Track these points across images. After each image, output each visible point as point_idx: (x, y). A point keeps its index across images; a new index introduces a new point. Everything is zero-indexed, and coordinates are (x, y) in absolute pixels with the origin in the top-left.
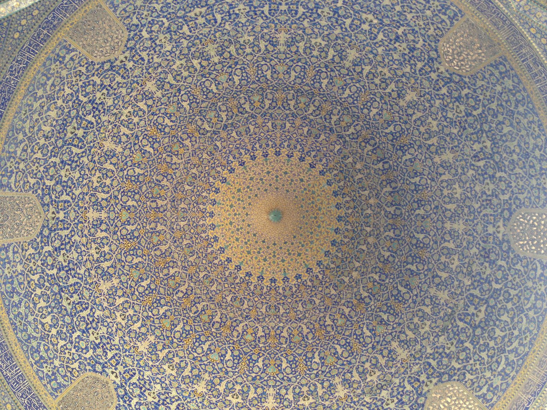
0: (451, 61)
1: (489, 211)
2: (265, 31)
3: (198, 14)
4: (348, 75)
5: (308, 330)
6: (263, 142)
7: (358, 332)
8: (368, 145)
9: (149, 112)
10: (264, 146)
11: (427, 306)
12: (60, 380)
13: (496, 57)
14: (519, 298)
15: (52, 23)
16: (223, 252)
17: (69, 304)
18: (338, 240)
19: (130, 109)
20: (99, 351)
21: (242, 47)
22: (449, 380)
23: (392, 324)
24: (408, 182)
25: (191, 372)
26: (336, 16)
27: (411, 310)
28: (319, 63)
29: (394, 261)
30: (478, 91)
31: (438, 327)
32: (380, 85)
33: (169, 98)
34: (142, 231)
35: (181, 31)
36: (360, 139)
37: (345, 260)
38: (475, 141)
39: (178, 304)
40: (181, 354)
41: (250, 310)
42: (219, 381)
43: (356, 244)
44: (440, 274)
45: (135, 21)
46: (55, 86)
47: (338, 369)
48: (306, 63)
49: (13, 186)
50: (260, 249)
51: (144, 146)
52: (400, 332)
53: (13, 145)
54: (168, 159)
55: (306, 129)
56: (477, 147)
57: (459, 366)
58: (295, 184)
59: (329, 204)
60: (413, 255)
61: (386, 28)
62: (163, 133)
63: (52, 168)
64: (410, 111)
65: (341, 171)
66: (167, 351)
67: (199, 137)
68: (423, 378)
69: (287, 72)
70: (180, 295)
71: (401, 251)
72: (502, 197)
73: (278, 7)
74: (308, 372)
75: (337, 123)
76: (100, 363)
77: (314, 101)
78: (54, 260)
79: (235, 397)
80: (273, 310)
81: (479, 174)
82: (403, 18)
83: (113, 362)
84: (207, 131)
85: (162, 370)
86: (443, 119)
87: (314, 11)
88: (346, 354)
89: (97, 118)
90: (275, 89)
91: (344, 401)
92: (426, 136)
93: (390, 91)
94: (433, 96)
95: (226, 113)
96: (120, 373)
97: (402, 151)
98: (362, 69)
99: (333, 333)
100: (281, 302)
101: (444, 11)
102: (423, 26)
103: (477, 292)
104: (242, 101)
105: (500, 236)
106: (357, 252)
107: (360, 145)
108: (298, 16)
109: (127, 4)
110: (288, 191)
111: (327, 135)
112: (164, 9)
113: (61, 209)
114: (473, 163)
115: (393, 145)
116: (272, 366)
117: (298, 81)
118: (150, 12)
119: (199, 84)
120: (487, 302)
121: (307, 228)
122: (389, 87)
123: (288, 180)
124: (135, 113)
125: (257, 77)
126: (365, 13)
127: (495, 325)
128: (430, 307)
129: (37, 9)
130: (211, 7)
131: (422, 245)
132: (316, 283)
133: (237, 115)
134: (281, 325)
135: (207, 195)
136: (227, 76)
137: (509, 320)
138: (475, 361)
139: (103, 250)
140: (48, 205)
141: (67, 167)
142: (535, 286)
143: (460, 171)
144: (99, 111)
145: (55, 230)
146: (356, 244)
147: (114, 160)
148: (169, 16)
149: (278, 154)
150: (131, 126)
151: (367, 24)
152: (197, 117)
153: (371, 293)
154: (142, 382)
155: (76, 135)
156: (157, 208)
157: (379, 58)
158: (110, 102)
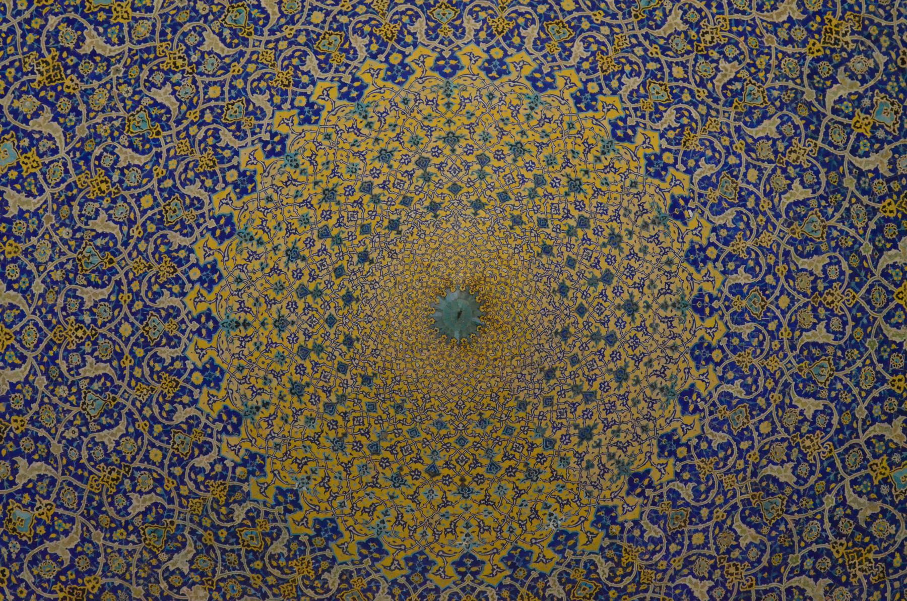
6: (753, 303)
10: (738, 303)
16: (345, 96)
41: (108, 172)
50: (338, 241)
55: (785, 474)
58: (574, 406)
67: (803, 57)
80: (96, 260)
84: (822, 91)
95: (884, 170)
100: (125, 297)
110: (550, 374)
111: (753, 554)
121: (397, 432)
123: (591, 380)
134: (38, 287)
135: (573, 61)
149: (701, 353)
152: (882, 59)
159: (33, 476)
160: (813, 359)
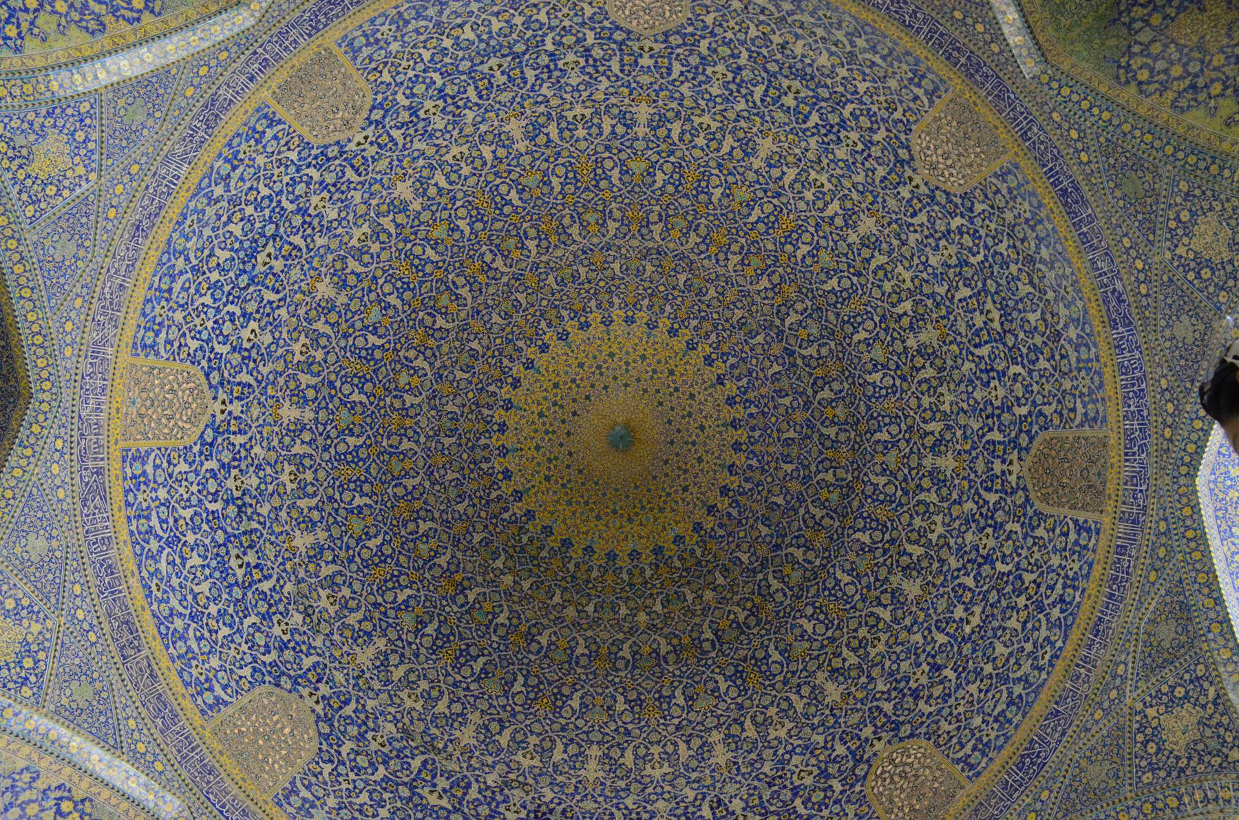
0: (892, 761)
2: (959, 433)
3: (990, 316)
4: (877, 579)
6: (760, 421)
7: (403, 580)
8: (746, 613)
9: (822, 219)
11: (449, 707)
12: (366, 51)
15: (977, 71)
16: (560, 339)
17: (491, 69)
18: (571, 553)
19: (828, 186)
20: (405, 116)
21: (932, 391)
22: (320, 734)
23: (418, 641)
24: (676, 684)
25: (352, 272)
26: (980, 560)
27: (441, 678)
28: (900, 528)
31: (412, 723)
32: (855, 638)
33: (846, 255)
34: (608, 194)
36: (758, 600)
37: (535, 562)
38: (747, 803)
39: (471, 253)
40: (385, 256)
42: (332, 321)
43: (563, 584)
44: (507, 733)
45: (979, 207)
46: (870, 67)
47: (341, 538)
48: (901, 504)
50: (562, 407)
51: (761, 205)
52: (403, 655)
54: (735, 248)
55: (780, 500)
57: (344, 754)
58: (679, 476)
59: (641, 537)
60: (542, 687)
61: (956, 648)
62: (783, 240)
63: (729, 52)
64: (805, 690)
65: (699, 563)
66: (393, 231)
67: (773, 305)
68: (324, 689)
69: (885, 470)
71: (549, 666)
73: (998, 457)
74: (337, 483)
76: (384, 117)
77: (832, 518)
78: (569, 47)
79: (304, 349)
81: (687, 808)
82: (972, 677)
83: (384, 139)
84: (783, 320)
85: (360, 221)
86: (789, 747)
87: (990, 522)
88: (366, 554)
89: (814, 130)
90: (856, 446)
91: (286, 545)
92: (760, 719)
94: (832, 730)
96: (364, 150)
97: (734, 675)
98: (885, 606)
99: (403, 533)
100: (464, 441)
101: (980, 746)
102: (955, 712)
103: (473, 794)
106: (550, 587)
107: (748, 600)
108: (982, 492)
110: (666, 462)
111: (768, 539)
112: (998, 257)
113: (656, 62)
114: (708, 798)
115: (745, 660)
116: (352, 419)
117: (869, 490)
118: (993, 233)
119: (869, 309)
122: (851, 654)
123: (686, 464)
125: (879, 415)
128: (447, 712)
129: (1002, 52)
130: (1001, 339)
131: (559, 703)
132: (495, 507)
133: (811, 375)
134: (423, 439)
135: (666, 314)
136: (882, 360)
138: (354, 781)
139: (580, 126)
140: (665, 41)
143: (694, 776)
144: (826, 135)
145: (621, 50)
146: (563, 584)
147: (738, 154)
148: (987, 265)
149: (737, 447)
150: (798, 186)
151: (964, 615)
153: (472, 607)
154: (344, 188)
155: (786, 94)
156: (648, 222)
157: (903, 635)
158: (841, 153)
159: (427, 528)
160: (789, 445)
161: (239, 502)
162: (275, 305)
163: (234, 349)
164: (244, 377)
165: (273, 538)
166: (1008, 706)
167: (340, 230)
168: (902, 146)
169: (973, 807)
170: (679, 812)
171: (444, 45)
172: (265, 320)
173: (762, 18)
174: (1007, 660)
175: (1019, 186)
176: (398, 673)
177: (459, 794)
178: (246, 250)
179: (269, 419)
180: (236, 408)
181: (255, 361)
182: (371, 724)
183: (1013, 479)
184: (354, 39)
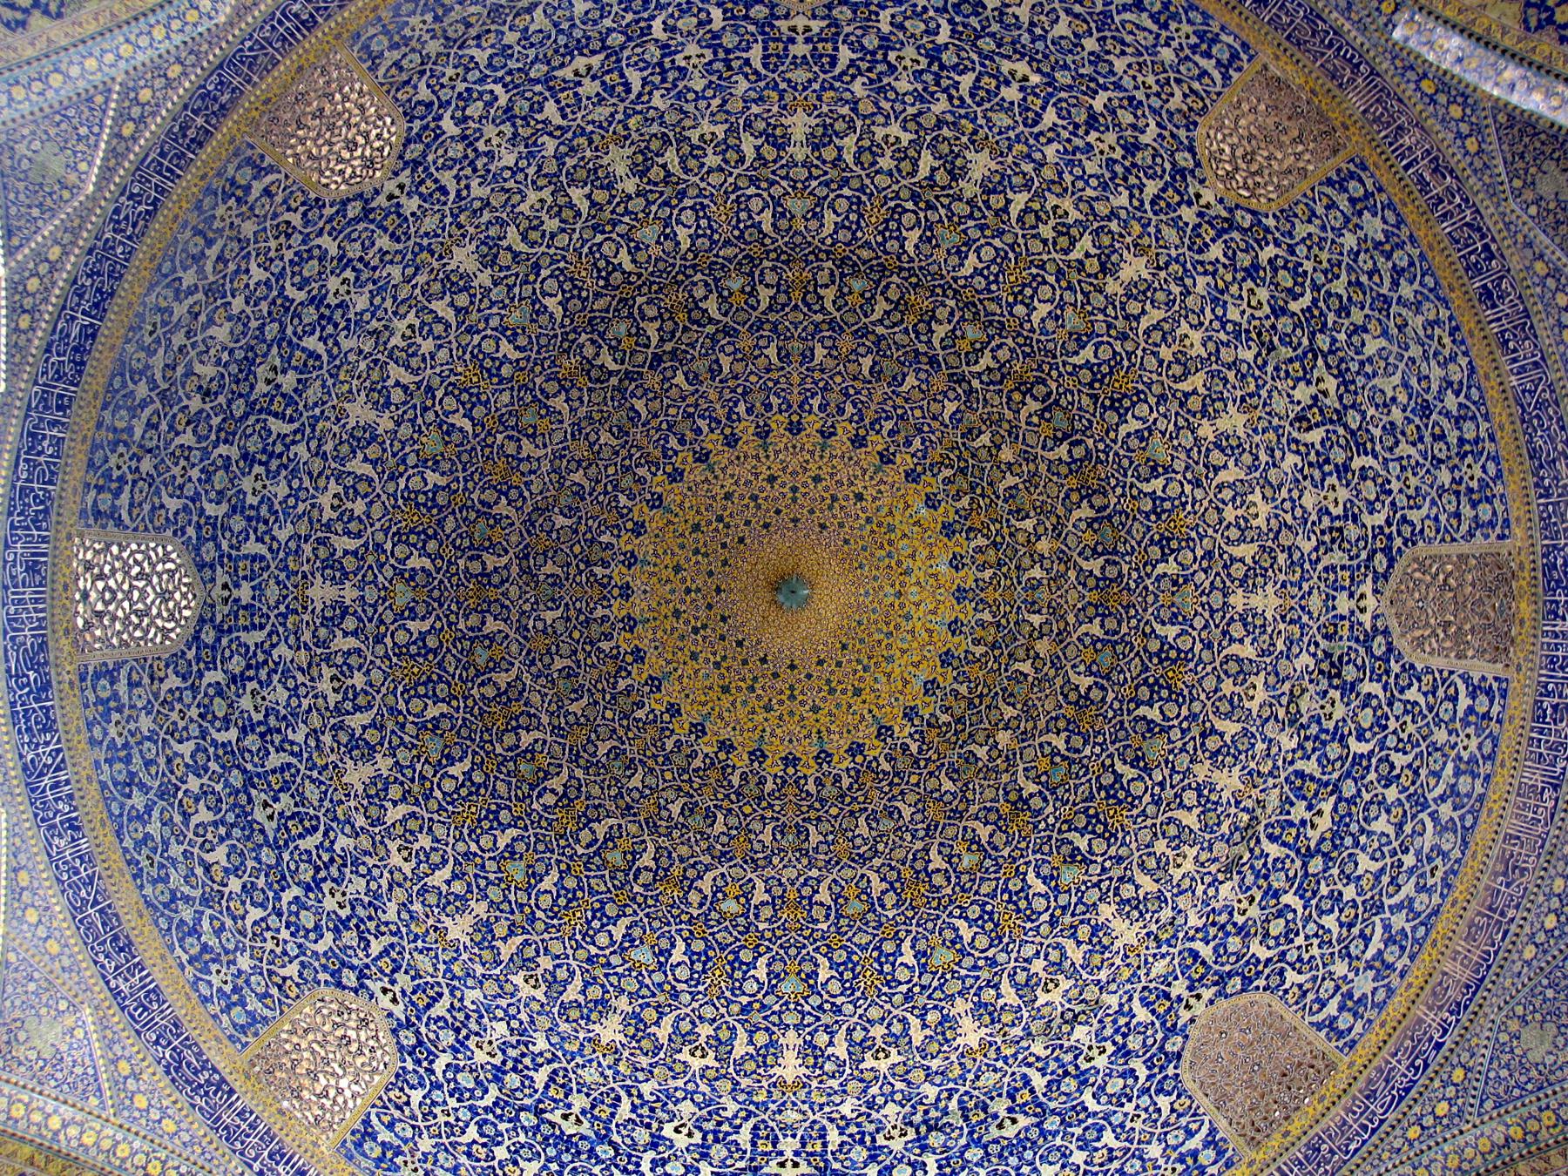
0: (1230, 176)
1: (1337, 557)
2: (755, 109)
3: (583, 71)
4: (971, 216)
5: (885, 885)
6: (757, 399)
7: (1015, 884)
8: (1028, 399)
11: (1190, 809)
12: (253, 1004)
13: (1340, 161)
14: (1416, 773)
17: (271, 817)
19: (411, 318)
20: (350, 937)
24: (1135, 492)
25: (583, 992)
26: (935, 68)
27: (1149, 822)
29: (1103, 699)
30: (1301, 250)
33: (510, 288)
34: (447, 635)
35: (539, 117)
36: (1009, 384)
38: (1299, 379)
40: (556, 948)
41: (732, 838)
42: (655, 1016)
44: (1220, 725)
45: (424, 93)
46: (226, 262)
48: (862, 189)
49: (125, 516)
50: (755, 679)
51: (447, 414)
52: (1120, 879)
53: (123, 413)
54: (511, 448)
55: (867, 362)
56: (1303, 393)
57: (1269, 954)
59: (931, 556)
61: (1063, 95)
63: (221, 473)
64: (1134, 308)
65: (962, 471)
66: (519, 940)
68: (1179, 988)
69: (815, 215)
70: (549, 799)
72: (1368, 520)
75: (948, 342)
76: (352, 968)
77: (887, 287)
78: (230, 706)
81: (1311, 465)
84: (611, 373)
85: (508, 988)
86: (1216, 325)
87: (879, 57)
88: (982, 942)
89: (330, 342)
91: (979, 1058)
92: (1177, 370)
93: (1080, 256)
95: (657, 325)
96: (403, 992)
98: (1008, 202)
100: (812, 814)
102: (1156, 88)
103: (1311, 767)
104: (699, 292)
105: (1366, 619)
107: (1009, 399)
108: (837, 71)
109: (404, 50)
110: (823, 526)
111: (923, 376)
112: (496, 61)
114: (1295, 434)
115: (1095, 398)
117: (844, 235)
120: (1336, 789)
121: (876, 622)
124: (425, 329)
126: (1009, 58)
127: (1356, 844)
128: (1196, 811)
130: (615, 53)
131: (1173, 654)
133: (686, 329)
134: (814, 873)
136: (657, 228)
137: (1391, 830)
138: (1307, 937)
139: (349, 682)
140: (212, 567)
141: (258, 469)
142: (1453, 739)
143: (1264, 458)
144: (336, 325)
145: (230, 631)
147: (373, 451)
149: (795, 428)
150: (414, 362)
151: (1015, 85)
153: (1045, 785)
154: (461, 1016)
155: (278, 386)
157: (1048, 173)
158: (361, 302)
161: (923, 1129)
162: (637, 1102)
163: (704, 1156)
164: (744, 1137)
165: (971, 1076)
166: (1144, 10)
167: (523, 1016)
168: (342, 211)
169: (1293, 49)
170: (1317, 474)
171: (238, 889)
172: (660, 1114)
173: (164, 427)
174: (1077, 16)
175: (386, 32)
176: (1147, 884)
177: (1313, 787)
178: (560, 1153)
179: (802, 1094)
180: (789, 1145)
181: (719, 1124)
182: (1223, 918)
183: (816, 26)
184: (235, 1025)
